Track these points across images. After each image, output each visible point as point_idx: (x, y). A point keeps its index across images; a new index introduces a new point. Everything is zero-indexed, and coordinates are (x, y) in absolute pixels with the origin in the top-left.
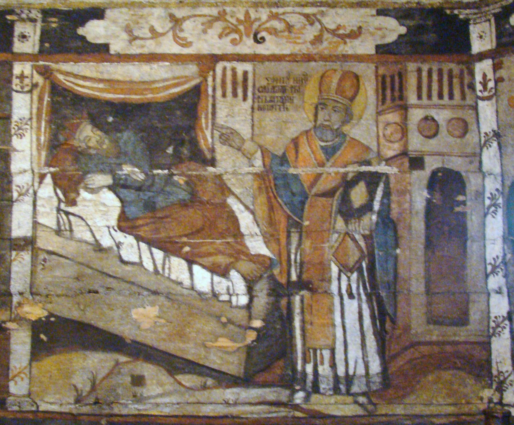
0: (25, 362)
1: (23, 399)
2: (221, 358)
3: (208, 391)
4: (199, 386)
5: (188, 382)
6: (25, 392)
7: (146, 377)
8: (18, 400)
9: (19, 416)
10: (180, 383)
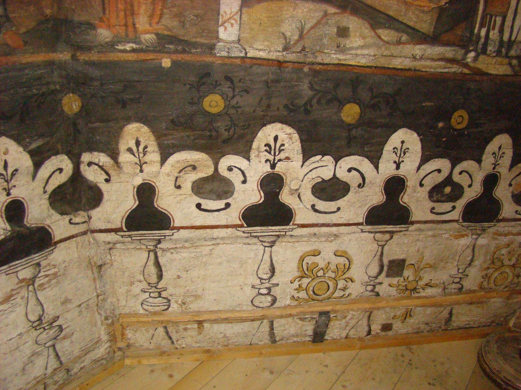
0: (236, 7)
1: (232, 45)
2: (418, 16)
3: (402, 46)
4: (395, 41)
5: (385, 36)
6: (234, 38)
7: (351, 29)
8: (228, 46)
9: (227, 61)
10: (379, 37)
